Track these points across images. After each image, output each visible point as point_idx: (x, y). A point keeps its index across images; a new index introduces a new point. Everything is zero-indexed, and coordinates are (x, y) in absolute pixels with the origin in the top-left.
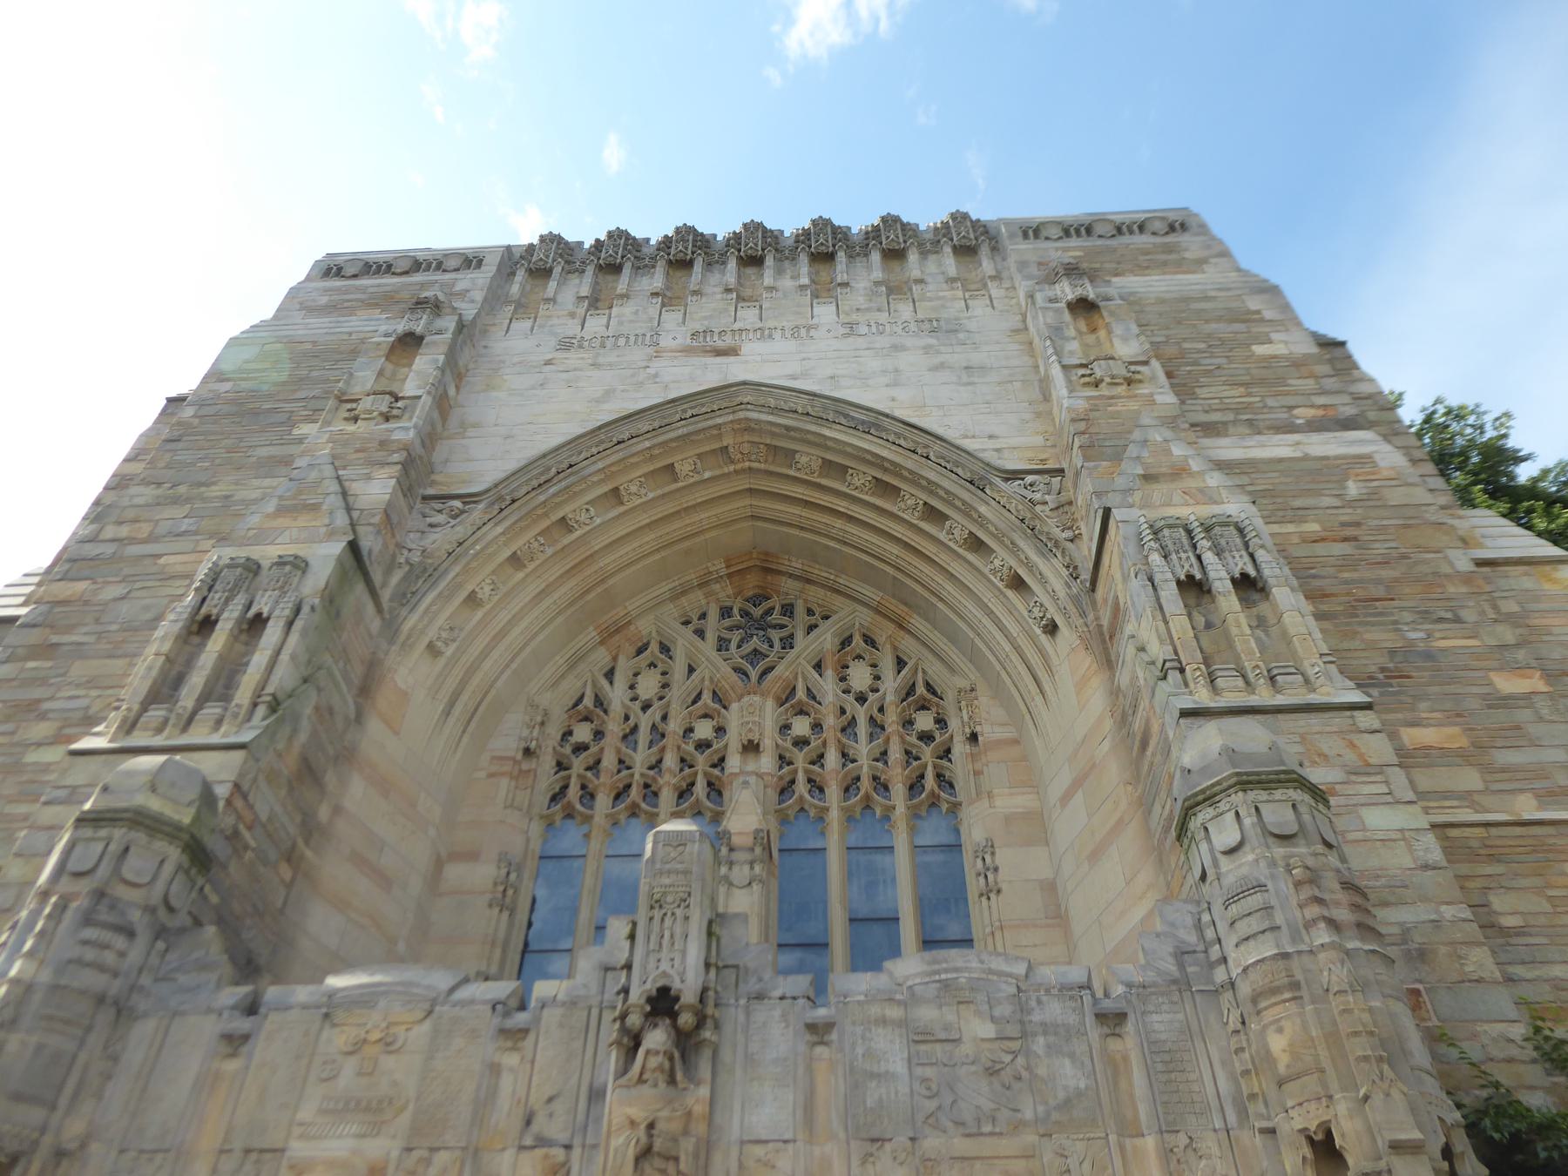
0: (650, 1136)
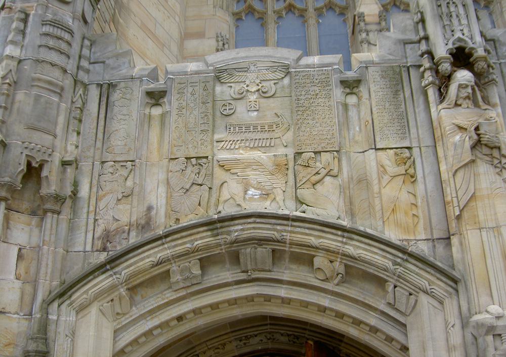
0: (478, 135)
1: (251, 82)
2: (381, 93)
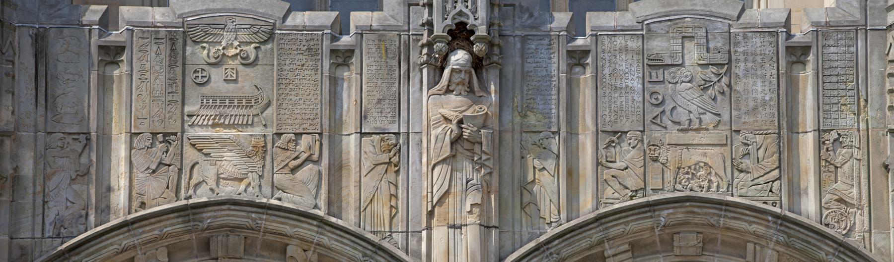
1: (230, 42)
2: (375, 67)
